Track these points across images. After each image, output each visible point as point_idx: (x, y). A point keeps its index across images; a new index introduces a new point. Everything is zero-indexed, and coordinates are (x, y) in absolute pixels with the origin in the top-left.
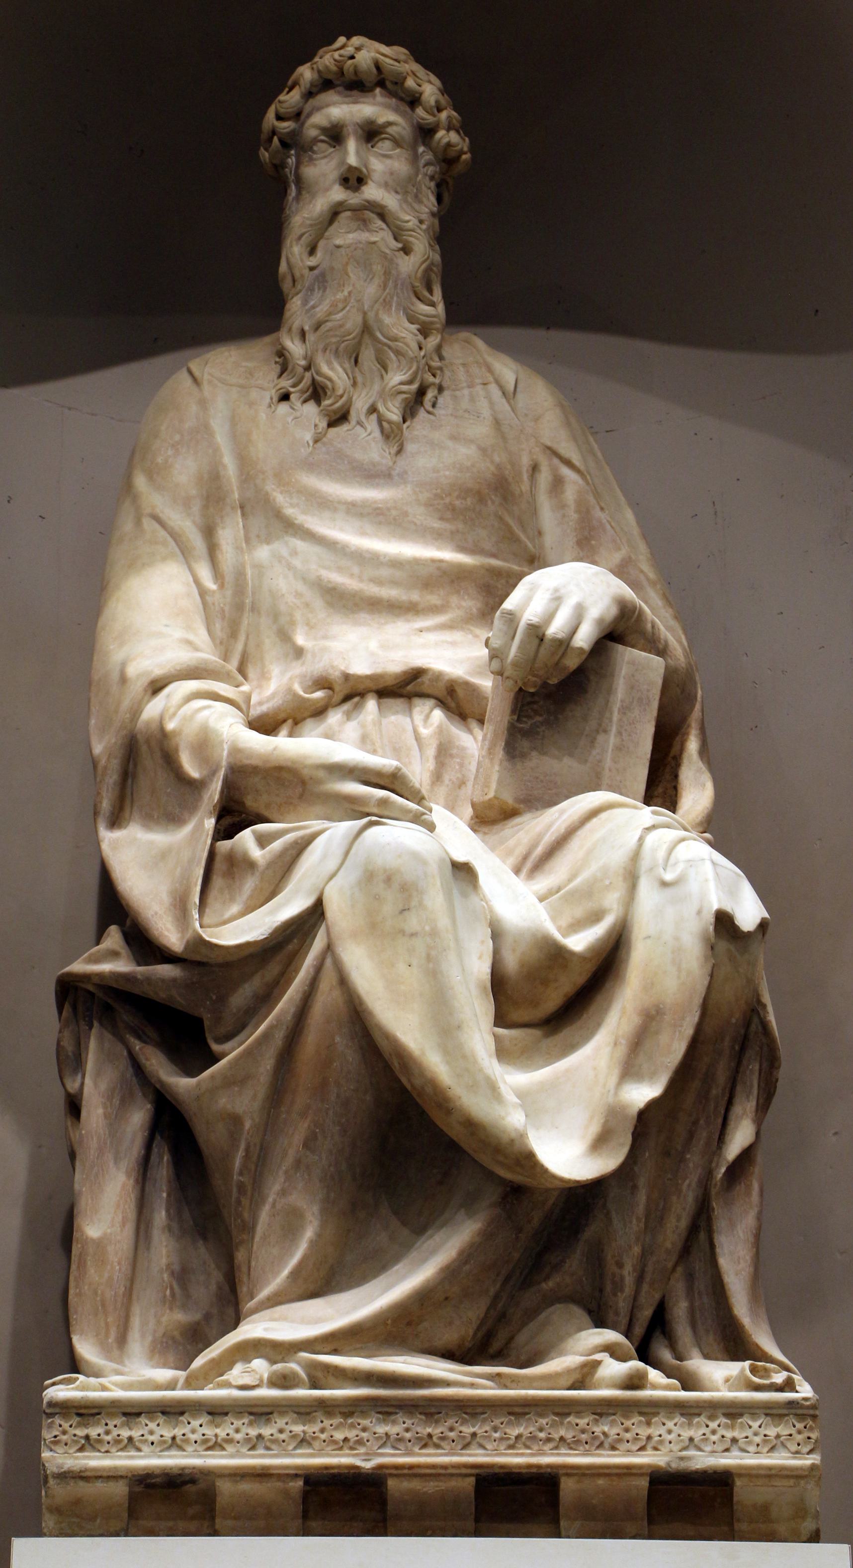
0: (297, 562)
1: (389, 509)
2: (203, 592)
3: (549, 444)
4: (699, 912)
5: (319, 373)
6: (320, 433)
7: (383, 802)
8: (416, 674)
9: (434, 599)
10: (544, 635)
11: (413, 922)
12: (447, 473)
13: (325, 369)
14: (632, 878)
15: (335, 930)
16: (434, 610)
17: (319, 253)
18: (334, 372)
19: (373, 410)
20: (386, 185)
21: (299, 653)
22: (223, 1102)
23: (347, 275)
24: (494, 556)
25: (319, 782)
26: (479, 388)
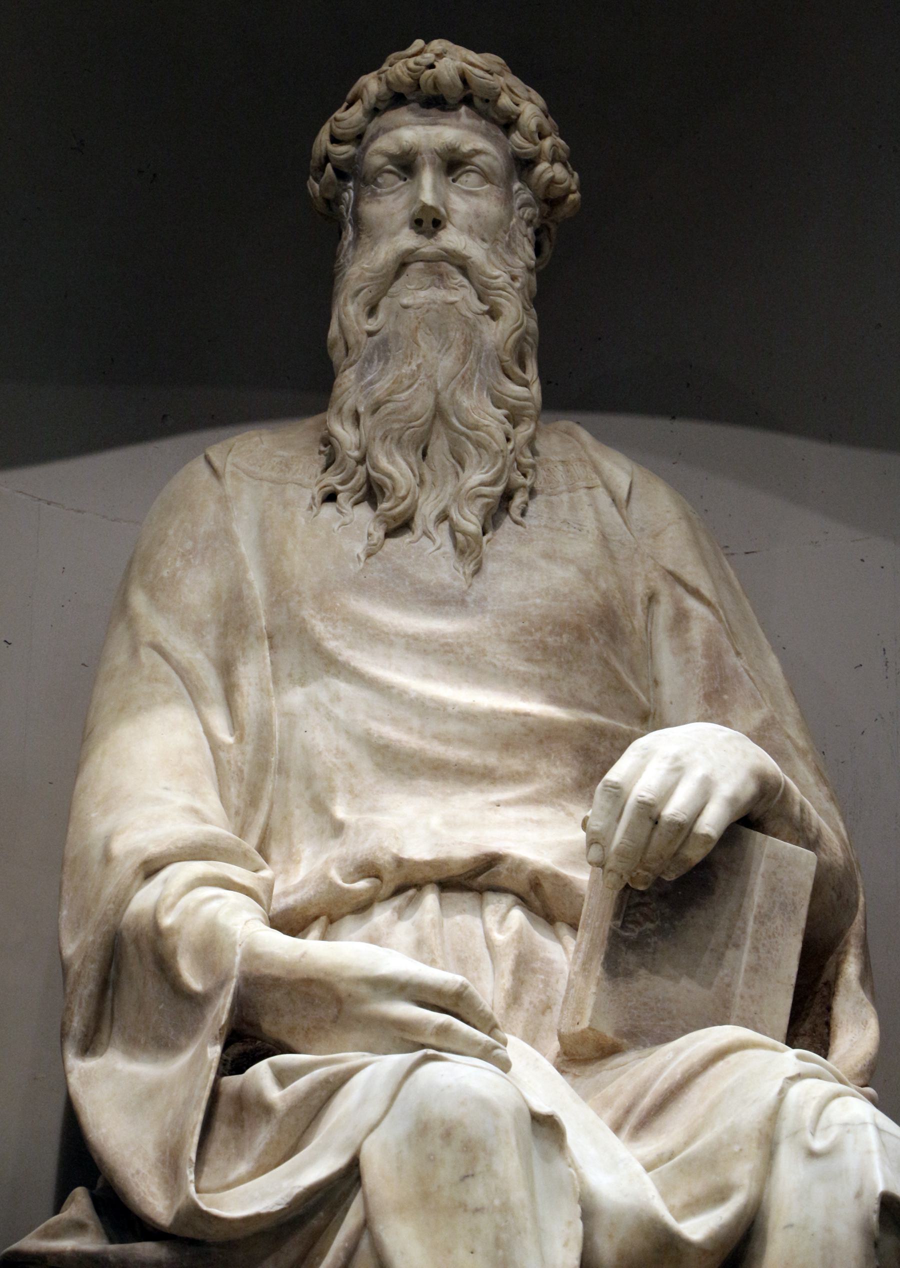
0: (339, 711)
1: (461, 647)
5: (375, 467)
6: (375, 545)
9: (516, 764)
10: (659, 816)
12: (538, 601)
16: (516, 778)
18: (396, 467)
19: (444, 516)
21: (338, 828)
24: (597, 710)
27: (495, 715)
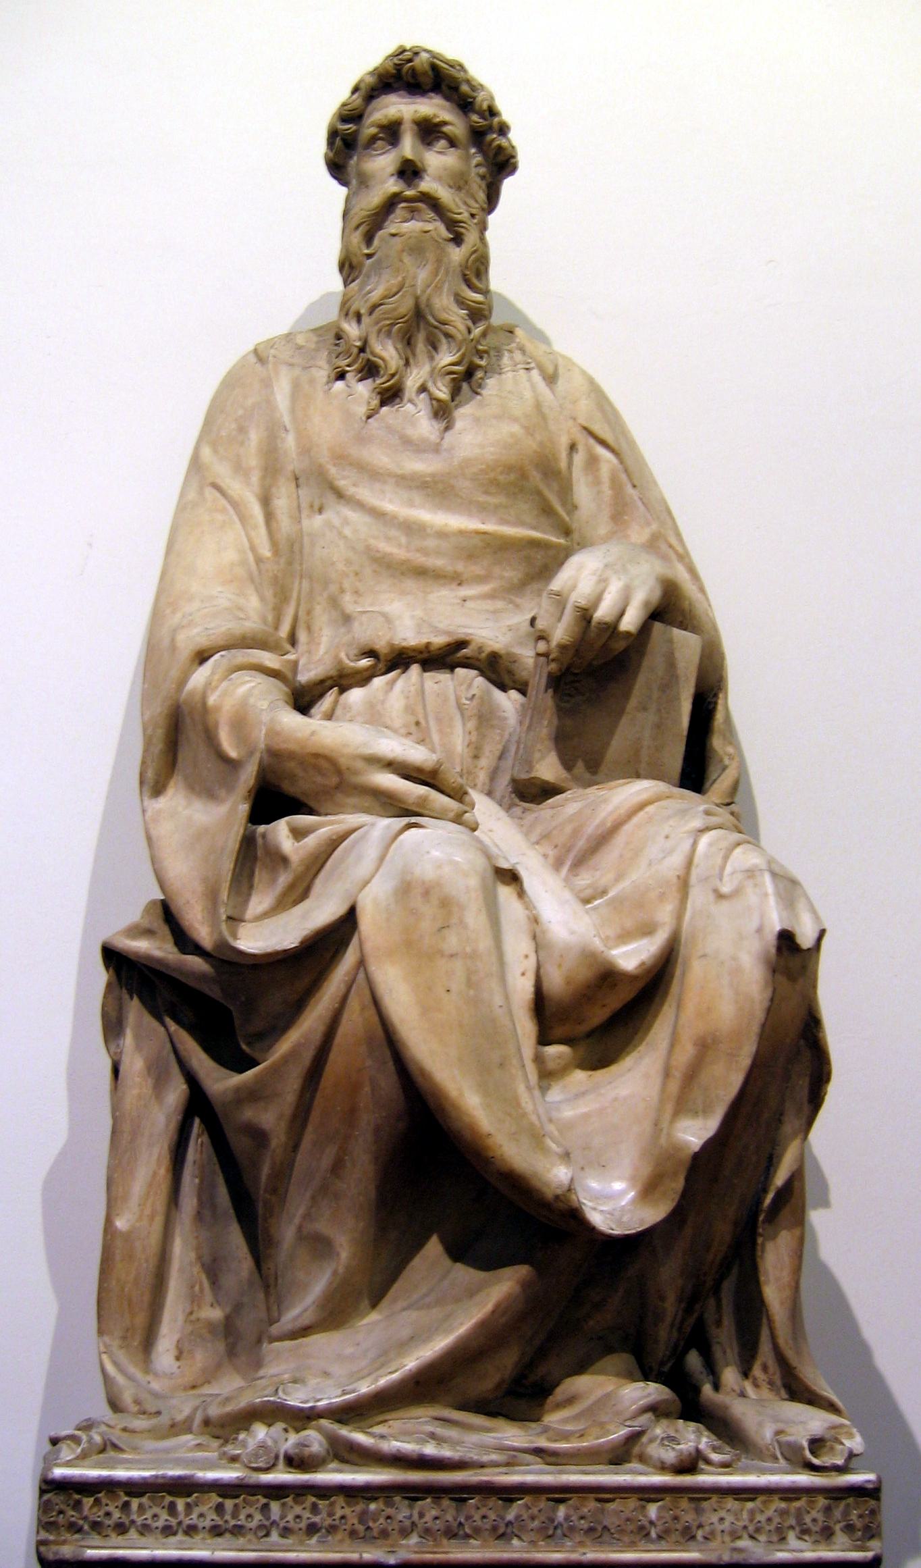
0: (347, 532)
1: (436, 483)
2: (259, 560)
3: (586, 425)
4: (759, 930)
7: (423, 800)
8: (461, 644)
9: (477, 569)
10: (591, 617)
11: (452, 941)
13: (378, 349)
14: (684, 884)
15: (369, 947)
17: (376, 242)
18: (388, 352)
19: (423, 389)
20: (439, 179)
21: (347, 619)
22: (249, 1114)
23: (401, 261)
24: (534, 528)
25: (356, 773)
26: (522, 372)
27: (461, 533)
